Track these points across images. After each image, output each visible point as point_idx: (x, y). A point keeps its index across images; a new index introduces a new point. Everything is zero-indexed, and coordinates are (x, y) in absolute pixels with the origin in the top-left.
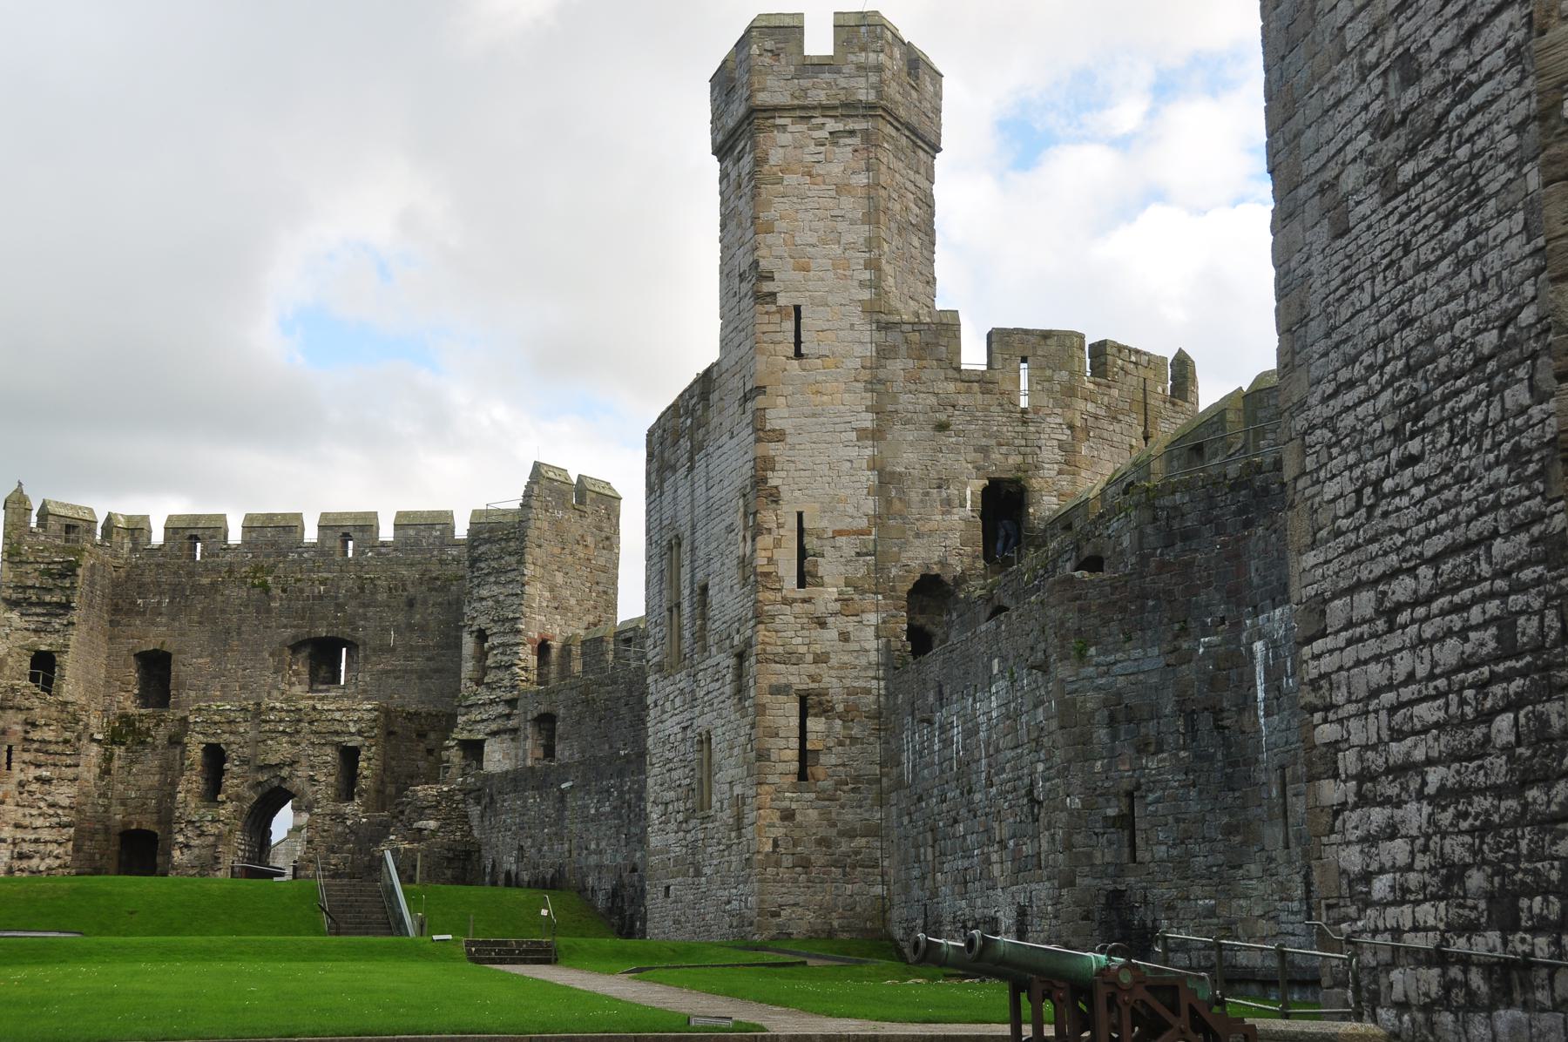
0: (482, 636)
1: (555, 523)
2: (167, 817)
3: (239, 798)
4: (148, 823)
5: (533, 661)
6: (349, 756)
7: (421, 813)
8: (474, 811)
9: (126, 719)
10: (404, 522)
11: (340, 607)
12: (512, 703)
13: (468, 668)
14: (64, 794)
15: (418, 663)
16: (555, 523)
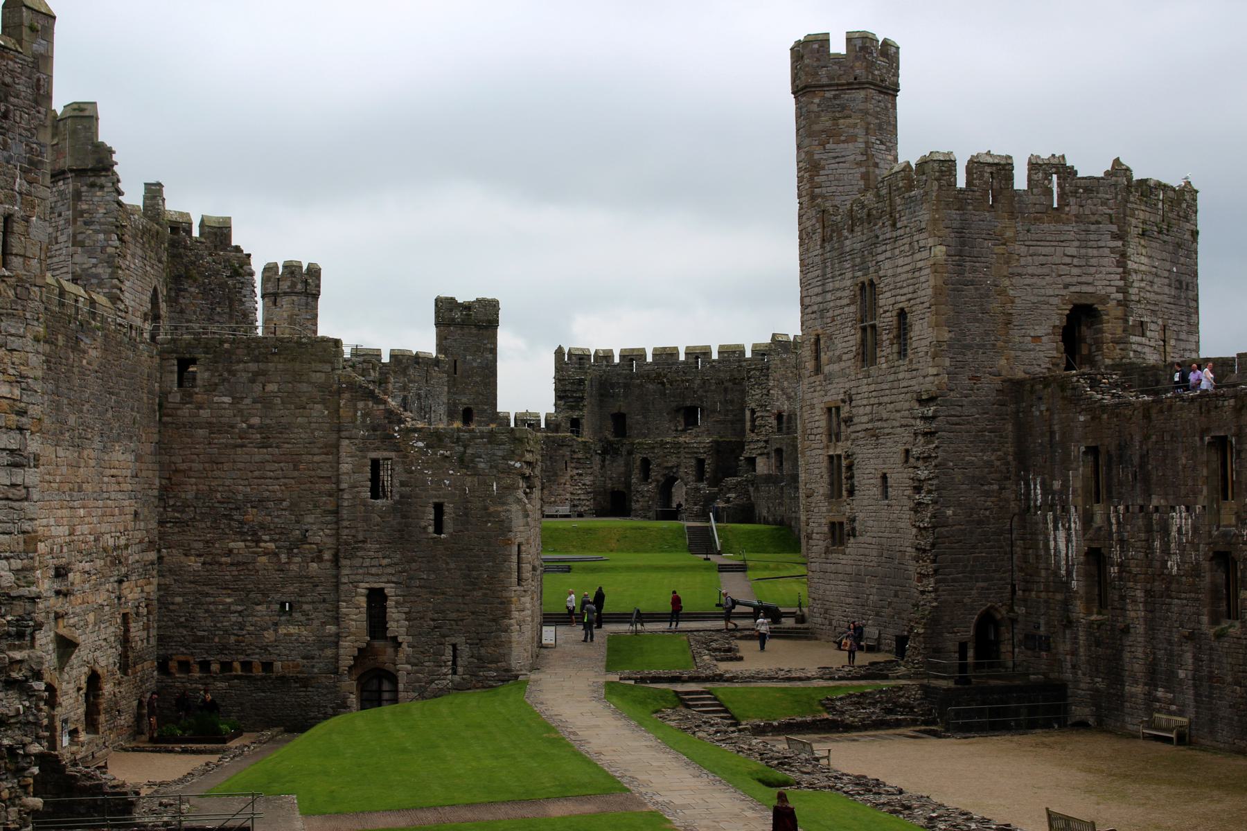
0: (753, 412)
1: (783, 360)
2: (628, 485)
3: (658, 481)
4: (621, 487)
5: (775, 423)
6: (701, 462)
7: (729, 490)
8: (751, 489)
9: (610, 443)
10: (723, 351)
11: (695, 392)
12: (766, 442)
13: (748, 424)
14: (588, 480)
15: (730, 417)
16: (783, 360)
